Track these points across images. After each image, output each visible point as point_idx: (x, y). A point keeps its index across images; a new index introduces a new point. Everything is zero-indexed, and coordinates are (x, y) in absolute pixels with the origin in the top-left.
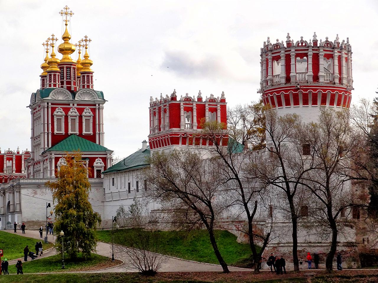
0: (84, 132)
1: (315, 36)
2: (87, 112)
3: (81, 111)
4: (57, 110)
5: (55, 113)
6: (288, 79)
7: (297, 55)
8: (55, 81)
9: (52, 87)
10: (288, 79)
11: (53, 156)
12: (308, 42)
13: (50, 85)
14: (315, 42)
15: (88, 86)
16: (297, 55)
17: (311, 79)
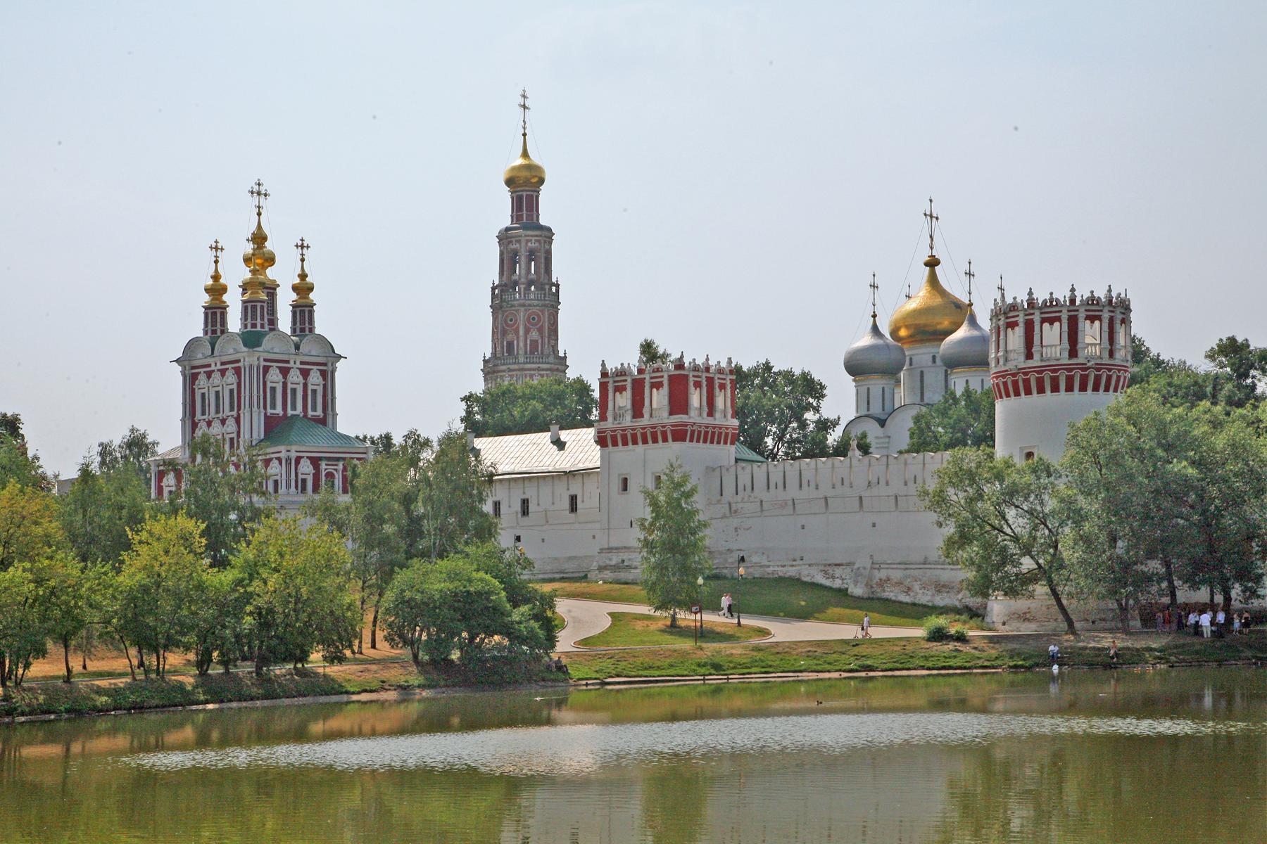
0: (310, 413)
1: (1073, 290)
2: (315, 378)
3: (305, 373)
4: (271, 371)
5: (269, 377)
6: (1029, 356)
7: (1043, 321)
8: (262, 319)
9: (259, 328)
10: (1029, 356)
11: (294, 455)
12: (1062, 300)
13: (254, 326)
14: (1073, 301)
15: (311, 330)
16: (1043, 321)
17: (1066, 354)
